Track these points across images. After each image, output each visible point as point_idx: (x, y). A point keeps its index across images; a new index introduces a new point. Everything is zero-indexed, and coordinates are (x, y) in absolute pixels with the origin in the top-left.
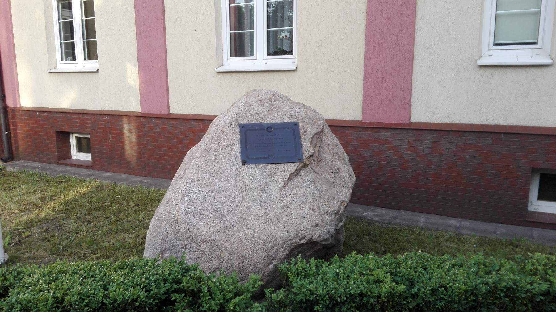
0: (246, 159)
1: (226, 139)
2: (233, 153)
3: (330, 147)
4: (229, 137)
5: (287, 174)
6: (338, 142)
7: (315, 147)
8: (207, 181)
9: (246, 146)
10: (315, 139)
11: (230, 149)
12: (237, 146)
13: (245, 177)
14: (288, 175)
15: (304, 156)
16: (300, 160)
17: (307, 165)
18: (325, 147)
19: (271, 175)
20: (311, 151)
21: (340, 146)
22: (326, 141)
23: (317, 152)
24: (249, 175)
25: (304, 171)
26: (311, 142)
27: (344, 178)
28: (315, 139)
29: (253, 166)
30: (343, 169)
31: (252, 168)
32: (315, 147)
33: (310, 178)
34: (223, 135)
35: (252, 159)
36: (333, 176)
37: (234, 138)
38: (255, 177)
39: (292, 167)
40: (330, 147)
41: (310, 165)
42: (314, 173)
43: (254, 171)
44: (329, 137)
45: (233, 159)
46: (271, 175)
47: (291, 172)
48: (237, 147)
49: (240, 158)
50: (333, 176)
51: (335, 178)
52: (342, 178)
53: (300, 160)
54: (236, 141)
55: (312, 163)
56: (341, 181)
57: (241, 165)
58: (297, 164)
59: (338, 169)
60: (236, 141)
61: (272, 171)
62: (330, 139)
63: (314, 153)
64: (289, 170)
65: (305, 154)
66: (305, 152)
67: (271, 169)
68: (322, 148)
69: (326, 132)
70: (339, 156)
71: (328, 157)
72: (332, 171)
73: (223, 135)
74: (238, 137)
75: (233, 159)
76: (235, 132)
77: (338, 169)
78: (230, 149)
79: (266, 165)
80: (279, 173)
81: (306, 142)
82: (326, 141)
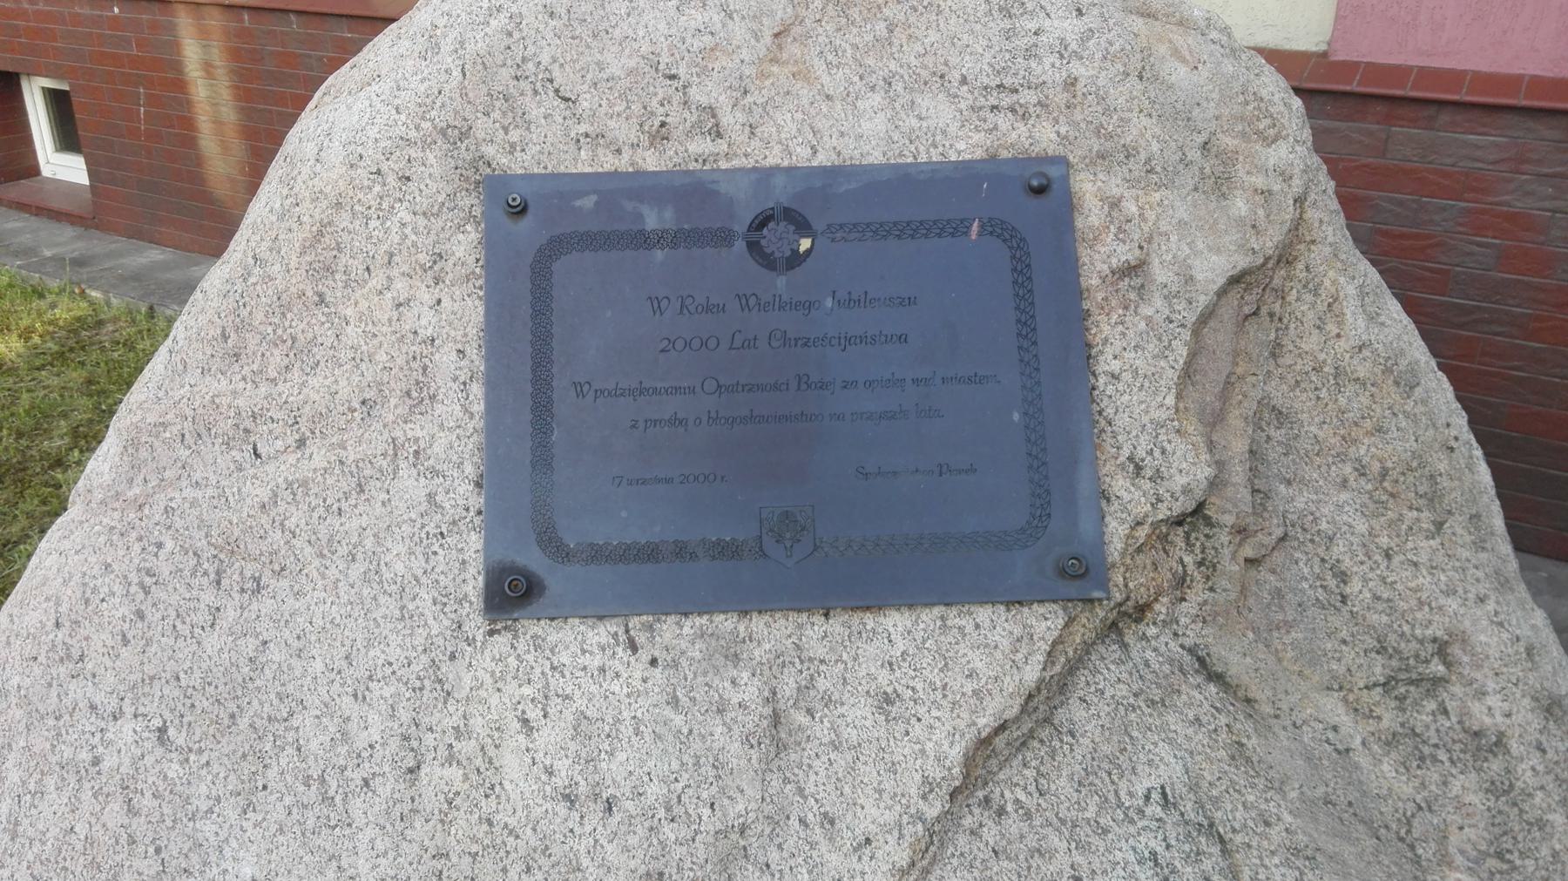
0: (533, 559)
1: (352, 333)
2: (411, 486)
3: (1354, 401)
4: (385, 312)
5: (941, 744)
6: (1418, 352)
7: (1214, 421)
8: (114, 813)
9: (542, 410)
10: (1219, 337)
11: (369, 442)
12: (449, 408)
13: (512, 765)
14: (956, 753)
15: (1116, 531)
16: (1076, 576)
17: (1142, 610)
18: (1301, 402)
19: (776, 734)
20: (1187, 470)
21: (1440, 391)
22: (1311, 343)
23: (1238, 474)
24: (549, 736)
25: (1110, 677)
26: (1188, 373)
27: (1500, 743)
28: (1219, 337)
29: (600, 633)
30: (1487, 639)
31: (578, 652)
32: (1214, 421)
33: (1170, 771)
34: (334, 289)
35: (597, 554)
36: (1389, 719)
37: (427, 323)
38: (616, 770)
39: (985, 653)
40: (1354, 401)
41: (1161, 608)
42: (1200, 696)
43: (612, 696)
44: (1350, 308)
45: (399, 561)
46: (776, 734)
47: (986, 722)
48: (454, 426)
49: (475, 541)
50: (1389, 719)
51: (1411, 747)
52: (1484, 745)
53: (1076, 576)
54: (445, 359)
55: (1181, 582)
56: (1466, 786)
57: (476, 624)
58: (1045, 622)
59: (1441, 650)
60: (445, 359)
61: (788, 685)
62: (1356, 324)
63: (1215, 484)
64: (959, 683)
65: (1128, 508)
66: (1120, 485)
67: (779, 660)
68: (1280, 416)
69: (1318, 255)
70: (1433, 499)
71: (1337, 510)
72: (1379, 672)
73: (334, 289)
74: (465, 312)
75: (399, 561)
76: (434, 268)
77: (1441, 650)
78: (376, 441)
79: (725, 623)
80: (859, 713)
81: (1135, 376)
82: (1311, 343)
